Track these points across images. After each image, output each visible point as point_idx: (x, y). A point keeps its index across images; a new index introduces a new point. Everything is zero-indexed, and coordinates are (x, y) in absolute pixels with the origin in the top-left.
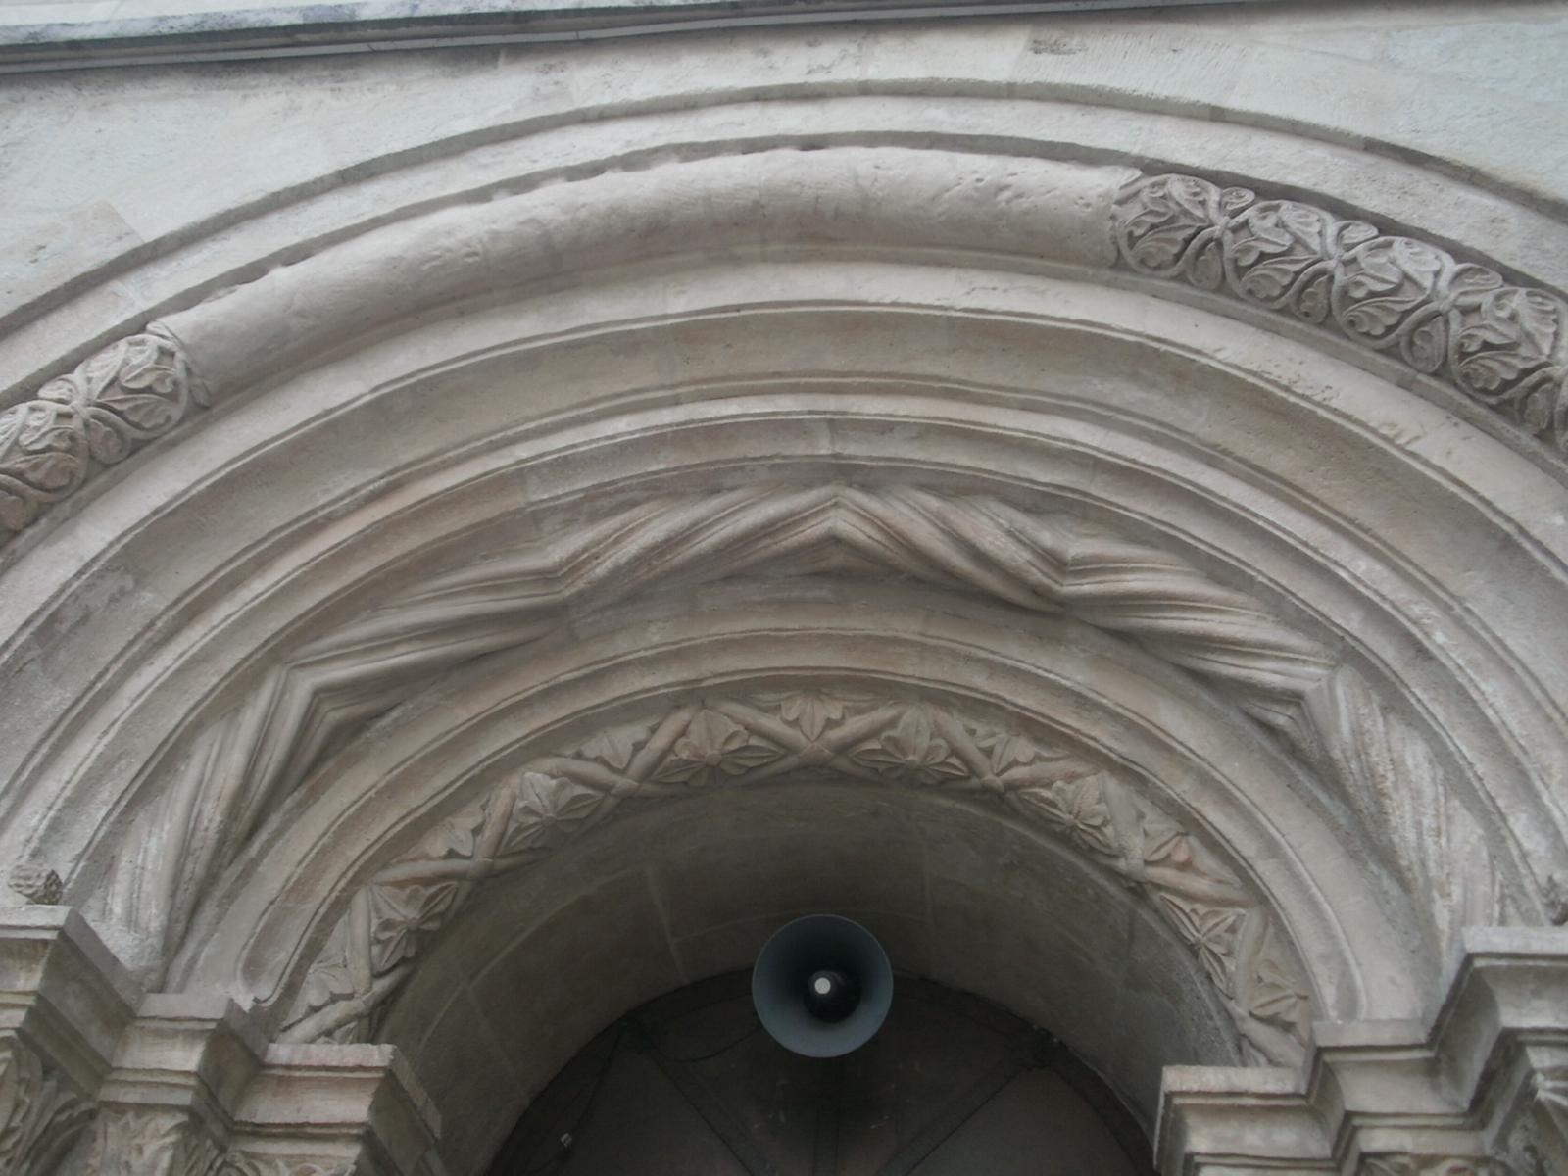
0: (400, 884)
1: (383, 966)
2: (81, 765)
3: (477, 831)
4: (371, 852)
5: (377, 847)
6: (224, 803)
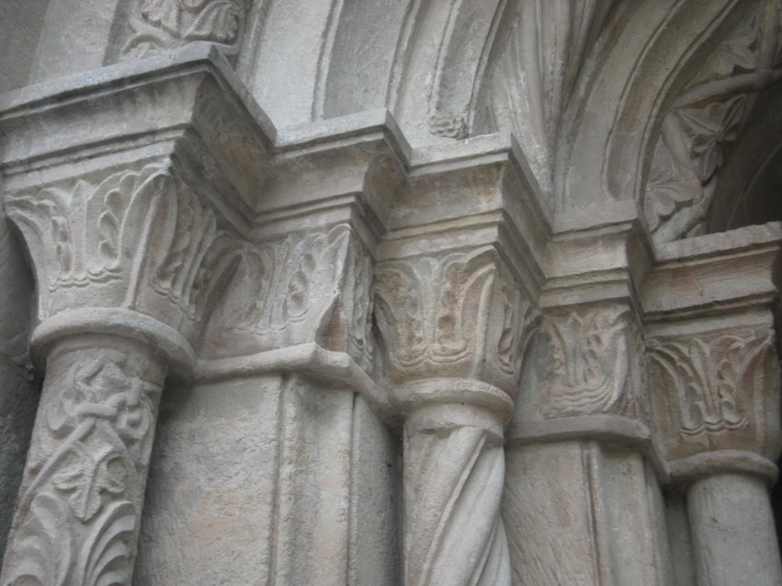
0: (698, 105)
1: (706, 176)
2: (445, 29)
3: (753, 47)
4: (671, 80)
5: (675, 74)
6: (561, 48)
